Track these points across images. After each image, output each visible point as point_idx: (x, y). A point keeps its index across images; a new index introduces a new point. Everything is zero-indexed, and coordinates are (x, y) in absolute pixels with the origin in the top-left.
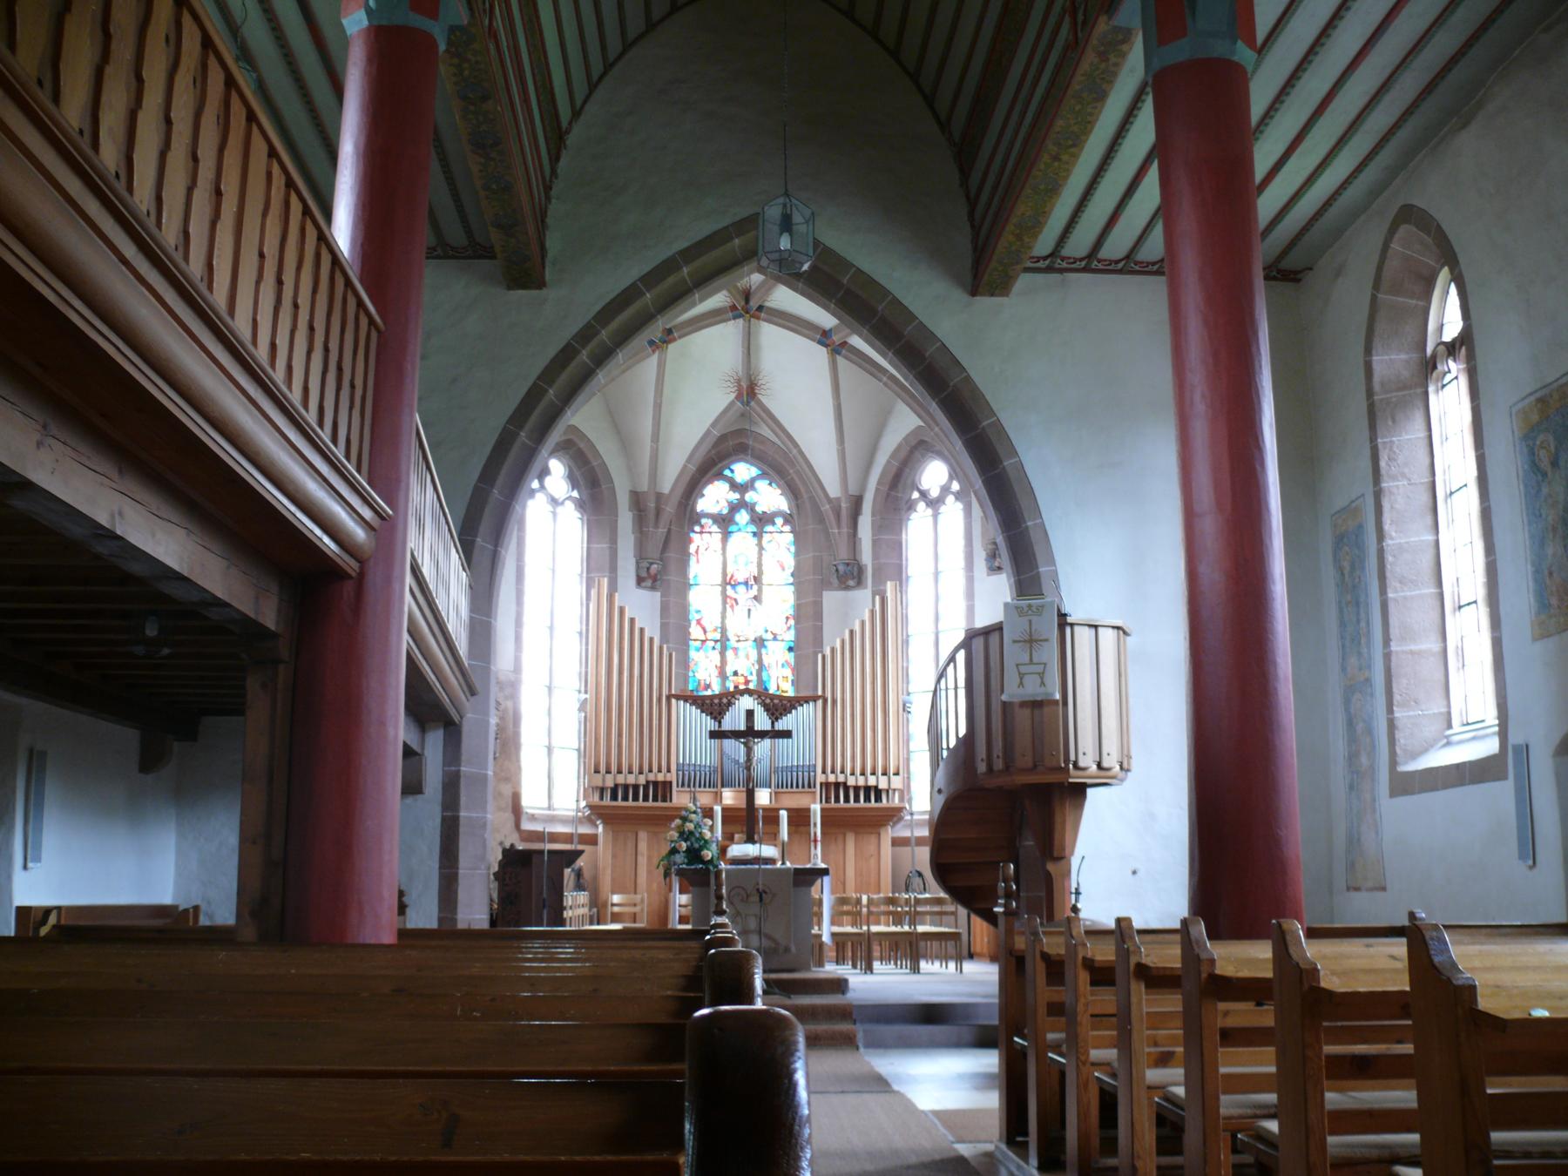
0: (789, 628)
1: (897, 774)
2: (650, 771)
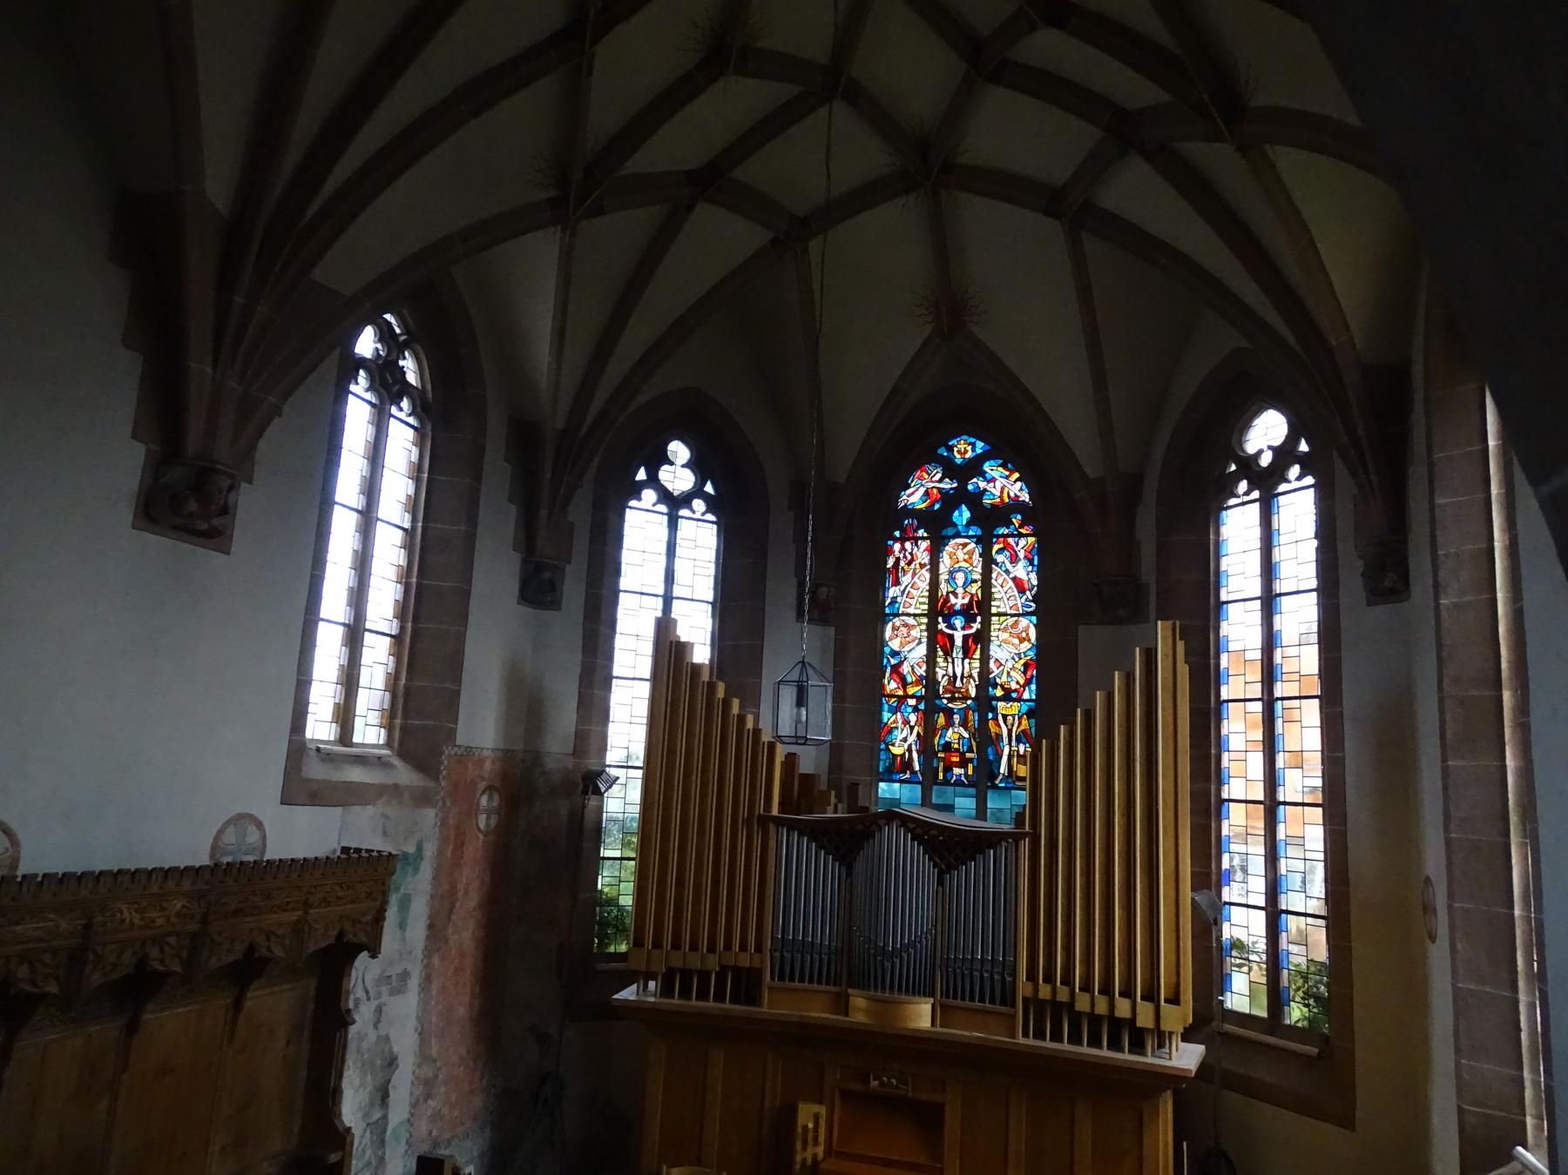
0: (1028, 682)
1: (1174, 1000)
2: (728, 947)
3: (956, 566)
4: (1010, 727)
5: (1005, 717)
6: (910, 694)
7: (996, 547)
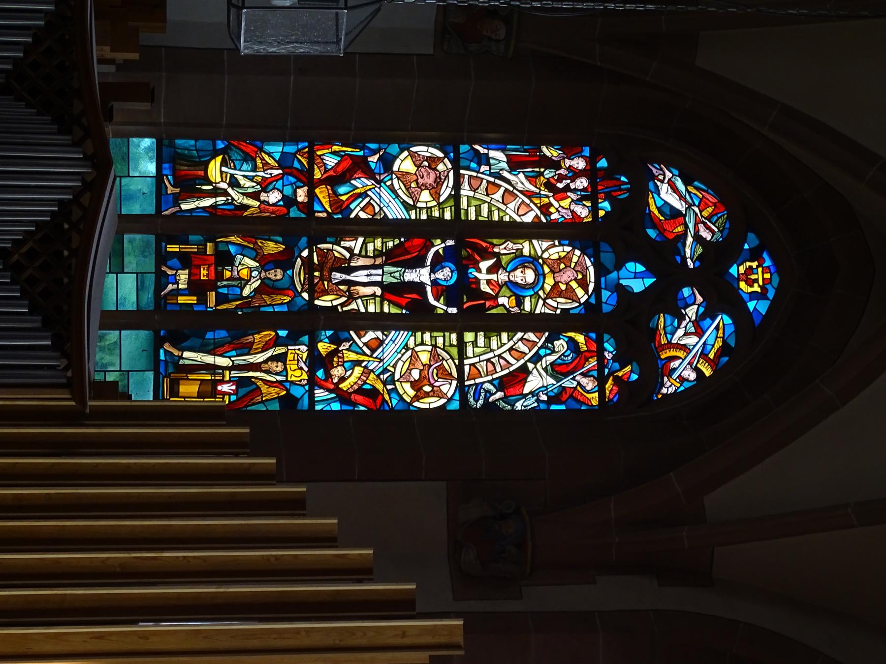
0: (343, 397)
3: (547, 270)
4: (265, 367)
5: (281, 358)
6: (317, 191)
7: (580, 338)
